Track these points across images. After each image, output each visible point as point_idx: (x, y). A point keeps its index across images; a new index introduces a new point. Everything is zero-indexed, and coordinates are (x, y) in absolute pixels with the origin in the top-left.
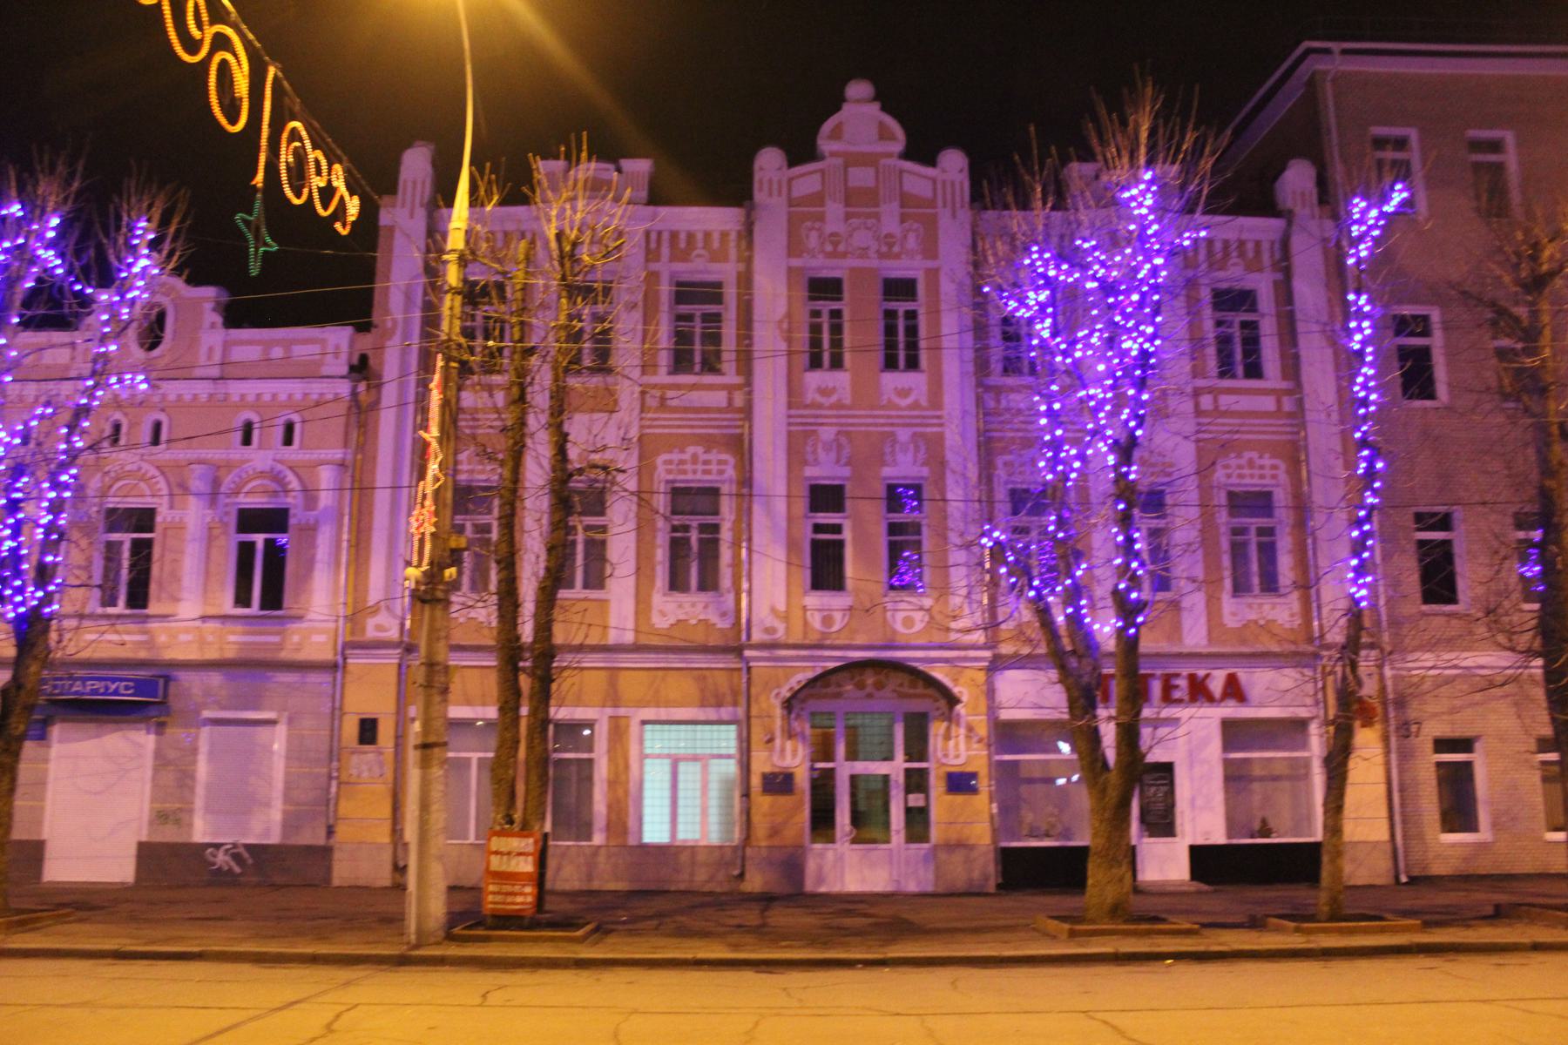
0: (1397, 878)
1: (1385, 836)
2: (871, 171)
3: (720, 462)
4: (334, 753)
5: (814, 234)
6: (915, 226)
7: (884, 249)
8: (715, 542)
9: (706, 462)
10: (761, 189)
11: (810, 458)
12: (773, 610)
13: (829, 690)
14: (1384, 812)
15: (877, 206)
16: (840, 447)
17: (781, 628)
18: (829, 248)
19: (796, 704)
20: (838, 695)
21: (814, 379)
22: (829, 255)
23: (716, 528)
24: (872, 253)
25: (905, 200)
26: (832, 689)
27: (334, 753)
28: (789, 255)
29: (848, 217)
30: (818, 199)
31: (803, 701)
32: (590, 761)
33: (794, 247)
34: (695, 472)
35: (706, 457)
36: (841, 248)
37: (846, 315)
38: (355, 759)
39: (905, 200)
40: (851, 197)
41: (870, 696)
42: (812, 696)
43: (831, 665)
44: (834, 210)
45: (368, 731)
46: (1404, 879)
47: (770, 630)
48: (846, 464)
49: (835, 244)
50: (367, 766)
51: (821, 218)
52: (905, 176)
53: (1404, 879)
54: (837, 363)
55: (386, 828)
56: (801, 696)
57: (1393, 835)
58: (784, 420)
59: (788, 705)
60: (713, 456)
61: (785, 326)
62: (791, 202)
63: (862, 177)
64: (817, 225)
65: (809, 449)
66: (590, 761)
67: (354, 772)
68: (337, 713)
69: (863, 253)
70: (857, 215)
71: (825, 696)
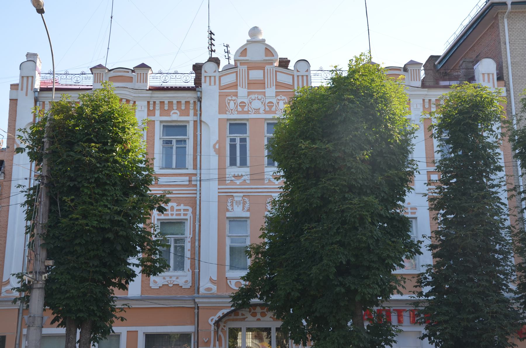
2: (261, 72)
3: (184, 210)
5: (232, 103)
6: (283, 98)
7: (267, 109)
8: (183, 248)
9: (177, 210)
10: (205, 82)
11: (230, 208)
12: (211, 280)
13: (238, 317)
16: (244, 203)
17: (214, 288)
18: (240, 109)
19: (222, 325)
20: (244, 319)
21: (231, 171)
22: (239, 112)
23: (183, 240)
24: (261, 111)
25: (279, 85)
26: (240, 317)
28: (220, 113)
29: (249, 94)
30: (235, 86)
31: (225, 323)
33: (222, 109)
34: (172, 215)
35: (179, 208)
36: (246, 109)
37: (248, 140)
39: (279, 85)
40: (251, 84)
41: (259, 320)
42: (229, 320)
44: (242, 91)
47: (209, 289)
48: (248, 210)
49: (243, 107)
51: (236, 95)
52: (278, 73)
54: (243, 163)
56: (224, 320)
58: (217, 191)
60: (182, 207)
61: (217, 147)
62: (221, 88)
63: (256, 75)
64: (234, 98)
65: (229, 204)
69: (257, 111)
70: (254, 93)
71: (236, 320)
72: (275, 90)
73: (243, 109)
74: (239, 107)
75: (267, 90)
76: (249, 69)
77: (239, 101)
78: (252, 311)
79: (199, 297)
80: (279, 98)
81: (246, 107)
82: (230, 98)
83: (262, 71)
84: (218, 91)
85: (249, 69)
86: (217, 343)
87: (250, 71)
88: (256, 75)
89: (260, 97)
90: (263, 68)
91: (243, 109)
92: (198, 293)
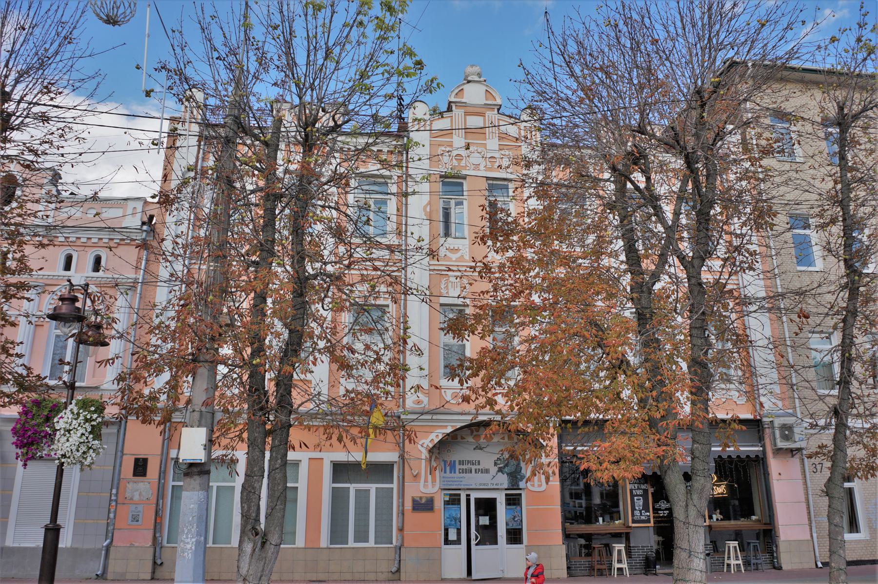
0: (816, 565)
1: (809, 538)
4: (116, 482)
14: (807, 522)
15: (485, 139)
24: (482, 167)
27: (116, 482)
32: (297, 488)
38: (130, 486)
43: (459, 425)
45: (140, 467)
46: (820, 565)
50: (141, 490)
53: (820, 565)
55: (149, 534)
57: (812, 536)
59: (431, 451)
61: (428, 209)
63: (475, 121)
66: (297, 488)
67: (128, 495)
68: (120, 452)
69: (477, 167)
72: (498, 143)
73: (459, 164)
74: (454, 161)
75: (488, 142)
76: (467, 114)
77: (454, 153)
78: (475, 433)
79: (404, 413)
80: (503, 152)
81: (464, 162)
82: (443, 148)
83: (482, 118)
84: (428, 138)
85: (467, 114)
86: (430, 477)
87: (468, 117)
88: (475, 121)
89: (479, 150)
90: (482, 115)
91: (459, 164)
92: (404, 407)
